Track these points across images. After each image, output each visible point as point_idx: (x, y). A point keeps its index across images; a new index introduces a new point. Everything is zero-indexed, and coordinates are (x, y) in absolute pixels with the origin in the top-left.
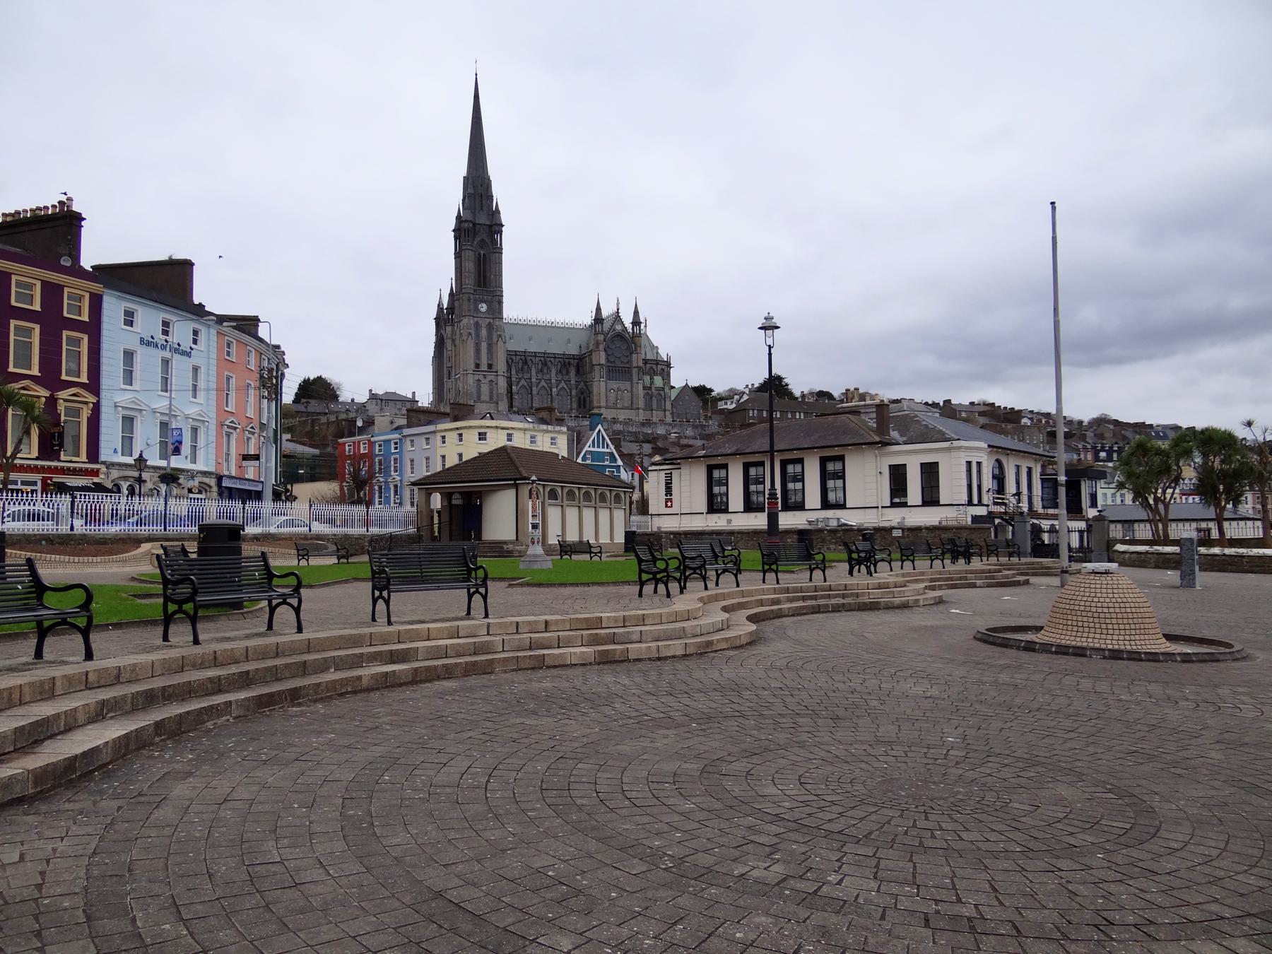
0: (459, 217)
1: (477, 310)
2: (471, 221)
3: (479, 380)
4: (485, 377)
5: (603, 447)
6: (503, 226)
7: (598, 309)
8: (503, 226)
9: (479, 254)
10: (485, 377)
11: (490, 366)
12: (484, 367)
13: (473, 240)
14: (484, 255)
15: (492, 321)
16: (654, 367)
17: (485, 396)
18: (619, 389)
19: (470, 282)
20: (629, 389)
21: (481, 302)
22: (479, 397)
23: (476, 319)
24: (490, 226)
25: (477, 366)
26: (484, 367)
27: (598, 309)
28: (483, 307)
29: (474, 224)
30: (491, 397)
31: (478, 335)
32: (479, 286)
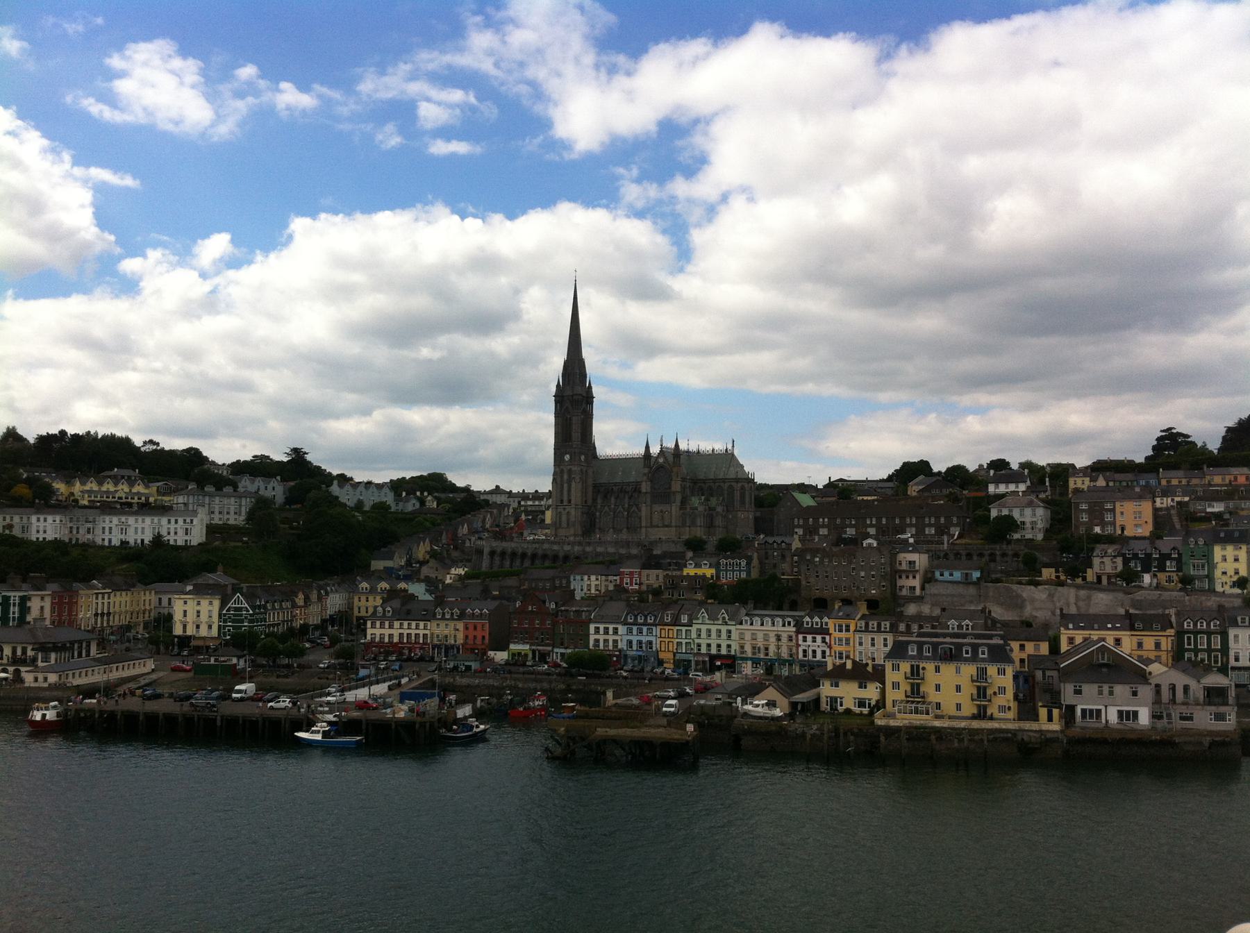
3: (560, 512)
4: (564, 509)
5: (238, 604)
7: (647, 447)
10: (564, 509)
16: (722, 484)
17: (564, 525)
18: (662, 511)
20: (669, 510)
21: (566, 454)
22: (560, 524)
24: (572, 396)
25: (562, 501)
27: (647, 447)
28: (567, 457)
29: (563, 397)
30: (568, 524)
31: (562, 480)
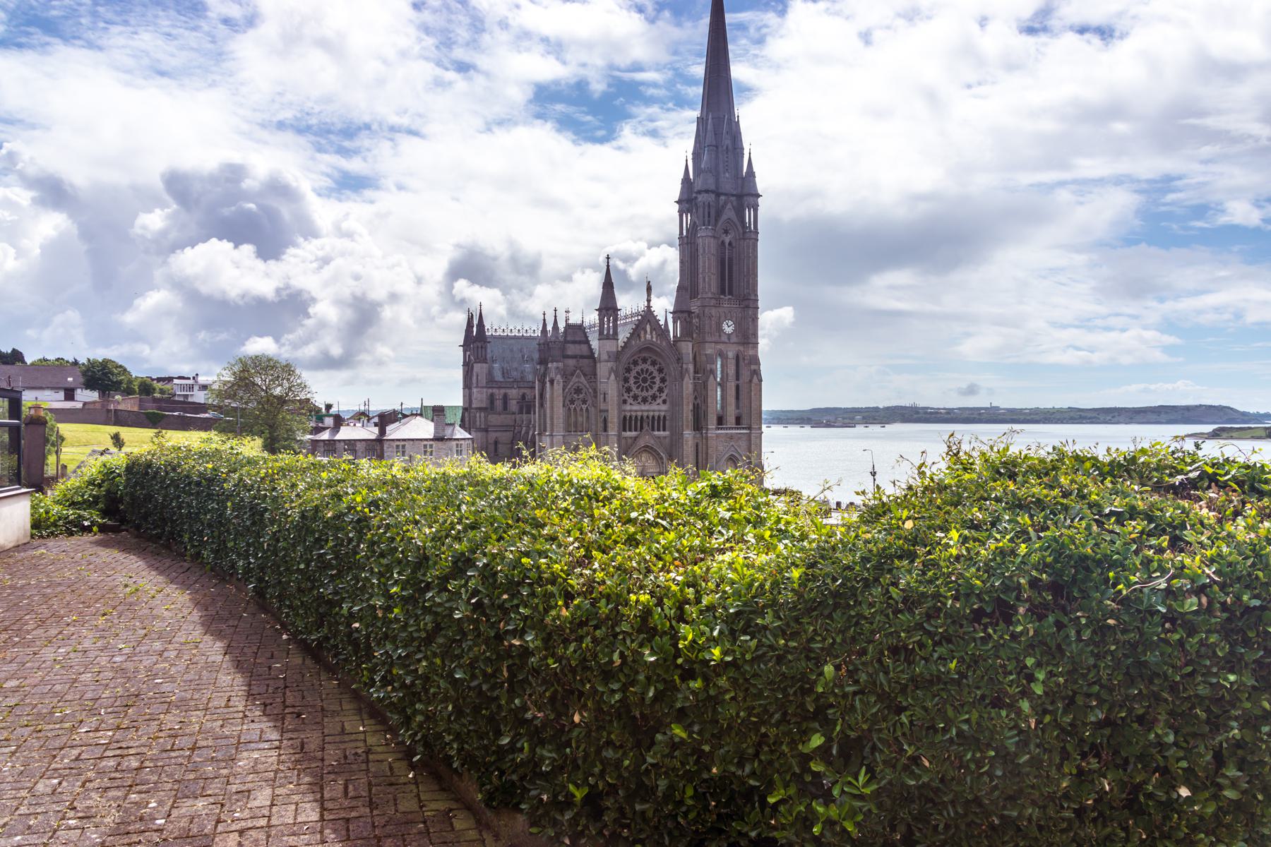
0: (686, 180)
1: (720, 329)
2: (712, 192)
6: (759, 196)
8: (759, 196)
9: (723, 243)
11: (738, 420)
12: (731, 419)
13: (715, 225)
14: (730, 244)
15: (741, 348)
19: (709, 280)
23: (719, 347)
26: (731, 419)
28: (728, 328)
32: (723, 292)
